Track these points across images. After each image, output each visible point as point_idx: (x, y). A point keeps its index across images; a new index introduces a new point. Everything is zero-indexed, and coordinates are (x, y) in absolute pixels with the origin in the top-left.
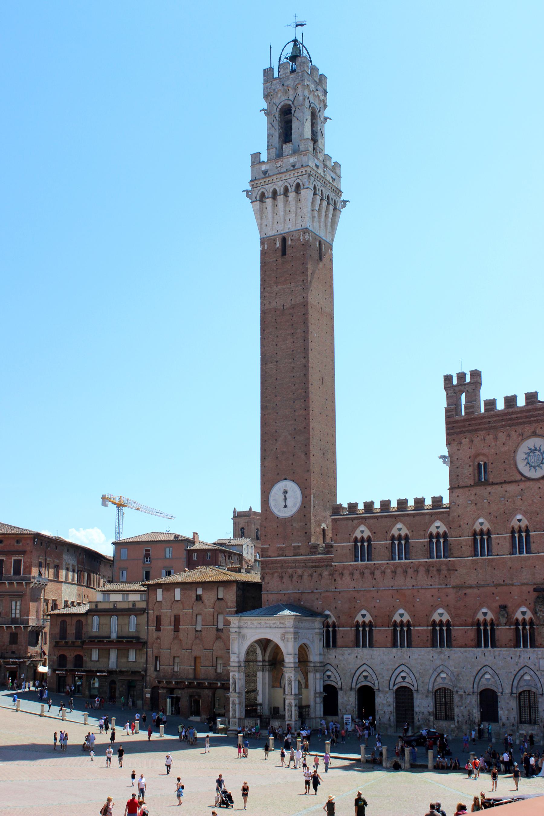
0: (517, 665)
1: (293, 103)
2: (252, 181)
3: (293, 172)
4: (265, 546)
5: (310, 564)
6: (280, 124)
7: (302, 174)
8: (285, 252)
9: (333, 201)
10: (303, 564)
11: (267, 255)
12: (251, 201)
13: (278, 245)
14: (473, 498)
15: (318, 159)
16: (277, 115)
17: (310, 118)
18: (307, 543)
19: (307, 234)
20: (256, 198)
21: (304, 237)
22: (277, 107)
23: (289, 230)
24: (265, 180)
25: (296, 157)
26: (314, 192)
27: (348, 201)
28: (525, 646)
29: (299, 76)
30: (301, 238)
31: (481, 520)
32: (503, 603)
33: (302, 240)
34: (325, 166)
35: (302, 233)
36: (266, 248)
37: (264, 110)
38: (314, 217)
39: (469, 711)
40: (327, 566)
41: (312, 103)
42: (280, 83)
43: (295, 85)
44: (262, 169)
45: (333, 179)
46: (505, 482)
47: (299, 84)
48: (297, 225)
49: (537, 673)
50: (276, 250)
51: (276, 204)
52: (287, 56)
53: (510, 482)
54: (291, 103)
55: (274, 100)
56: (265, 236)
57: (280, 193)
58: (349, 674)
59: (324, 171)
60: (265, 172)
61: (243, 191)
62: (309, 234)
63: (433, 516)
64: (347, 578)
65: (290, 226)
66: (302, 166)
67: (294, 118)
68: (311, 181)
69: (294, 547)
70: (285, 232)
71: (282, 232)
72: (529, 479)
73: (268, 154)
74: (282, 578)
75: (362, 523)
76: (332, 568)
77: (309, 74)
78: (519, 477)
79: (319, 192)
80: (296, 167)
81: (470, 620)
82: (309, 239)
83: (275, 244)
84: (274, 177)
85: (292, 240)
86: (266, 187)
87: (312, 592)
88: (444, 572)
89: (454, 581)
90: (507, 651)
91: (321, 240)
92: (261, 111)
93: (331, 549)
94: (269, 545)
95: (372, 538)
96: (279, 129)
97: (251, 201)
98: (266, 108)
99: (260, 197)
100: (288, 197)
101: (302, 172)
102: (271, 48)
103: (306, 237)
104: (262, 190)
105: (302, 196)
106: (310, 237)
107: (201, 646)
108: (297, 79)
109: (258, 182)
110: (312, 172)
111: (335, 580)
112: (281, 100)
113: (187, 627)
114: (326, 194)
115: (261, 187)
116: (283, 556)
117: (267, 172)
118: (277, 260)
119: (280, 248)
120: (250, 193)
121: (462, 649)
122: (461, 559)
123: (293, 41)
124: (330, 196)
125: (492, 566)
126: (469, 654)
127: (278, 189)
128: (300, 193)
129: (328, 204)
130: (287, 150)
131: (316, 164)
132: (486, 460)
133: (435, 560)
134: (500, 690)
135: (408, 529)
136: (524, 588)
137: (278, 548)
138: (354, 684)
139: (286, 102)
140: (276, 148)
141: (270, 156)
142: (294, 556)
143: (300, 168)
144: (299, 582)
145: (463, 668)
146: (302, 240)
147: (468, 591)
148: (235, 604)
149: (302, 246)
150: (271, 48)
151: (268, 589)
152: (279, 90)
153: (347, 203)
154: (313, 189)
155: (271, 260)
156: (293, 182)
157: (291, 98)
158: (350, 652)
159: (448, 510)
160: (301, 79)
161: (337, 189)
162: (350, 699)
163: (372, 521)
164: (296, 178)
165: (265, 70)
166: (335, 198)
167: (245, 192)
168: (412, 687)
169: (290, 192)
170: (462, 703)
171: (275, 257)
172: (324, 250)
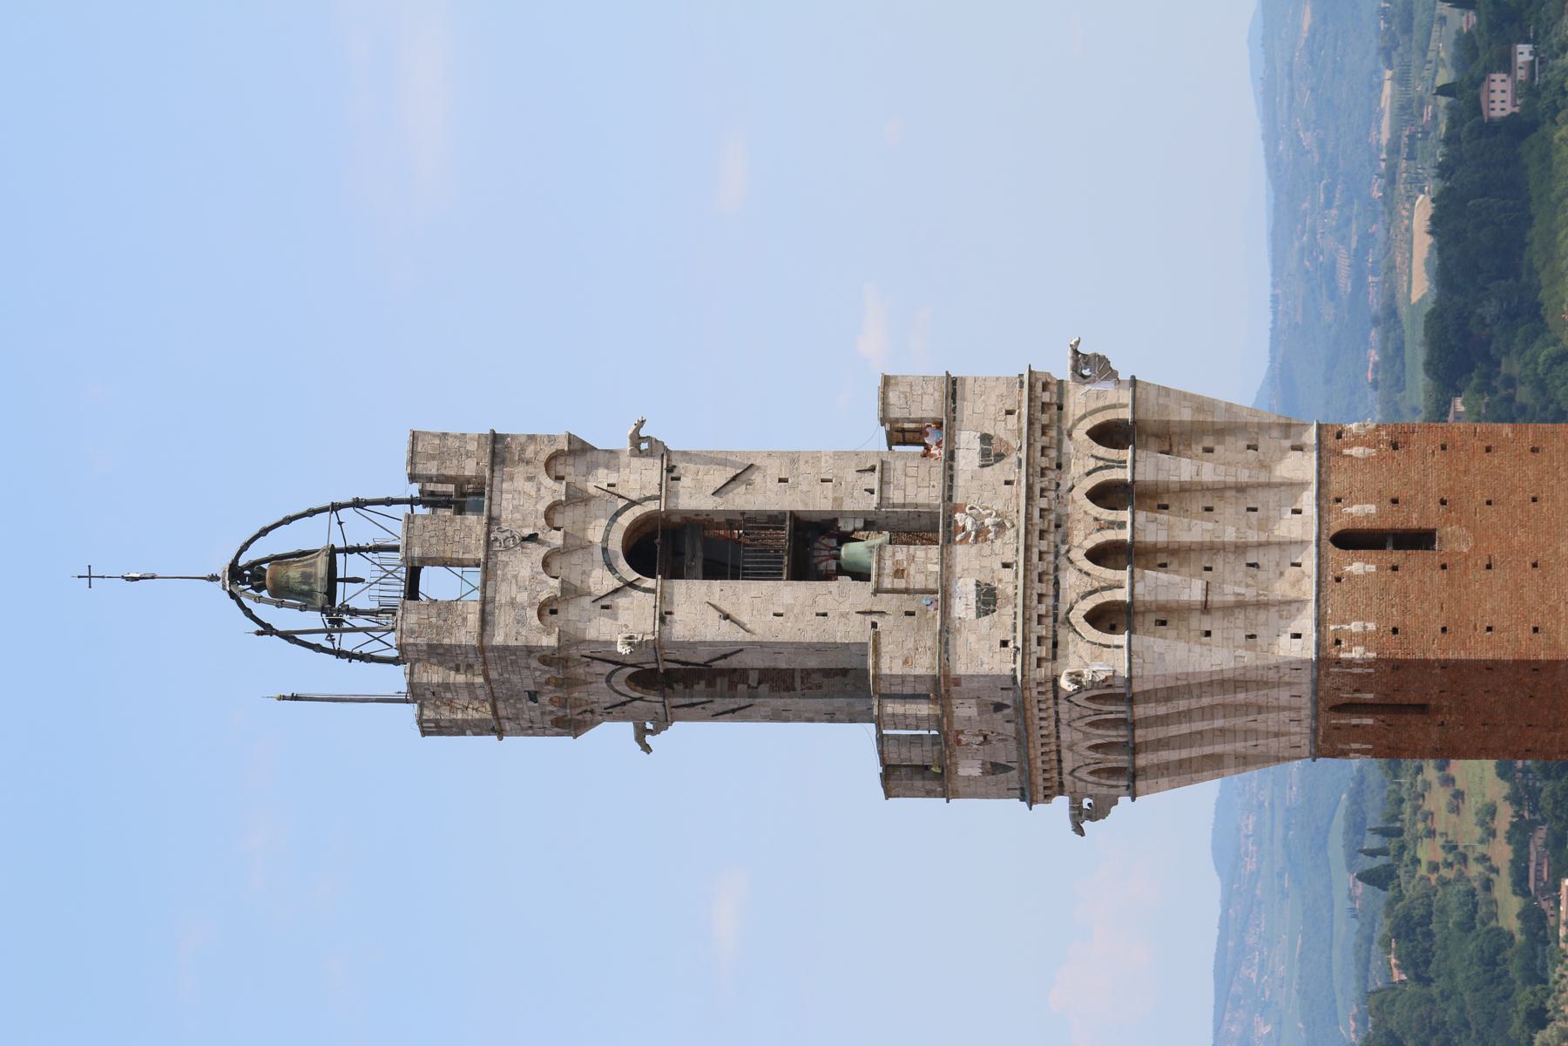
2: (1028, 795)
12: (1124, 801)
13: (1369, 721)
27: (1076, 352)
38: (1241, 605)
61: (1079, 830)
79: (1118, 584)
82: (1363, 638)
92: (647, 748)
97: (1124, 801)
98: (627, 728)
102: (295, 698)
120: (1086, 802)
150: (295, 698)
154: (1121, 639)
167: (1086, 825)
172: (1371, 508)
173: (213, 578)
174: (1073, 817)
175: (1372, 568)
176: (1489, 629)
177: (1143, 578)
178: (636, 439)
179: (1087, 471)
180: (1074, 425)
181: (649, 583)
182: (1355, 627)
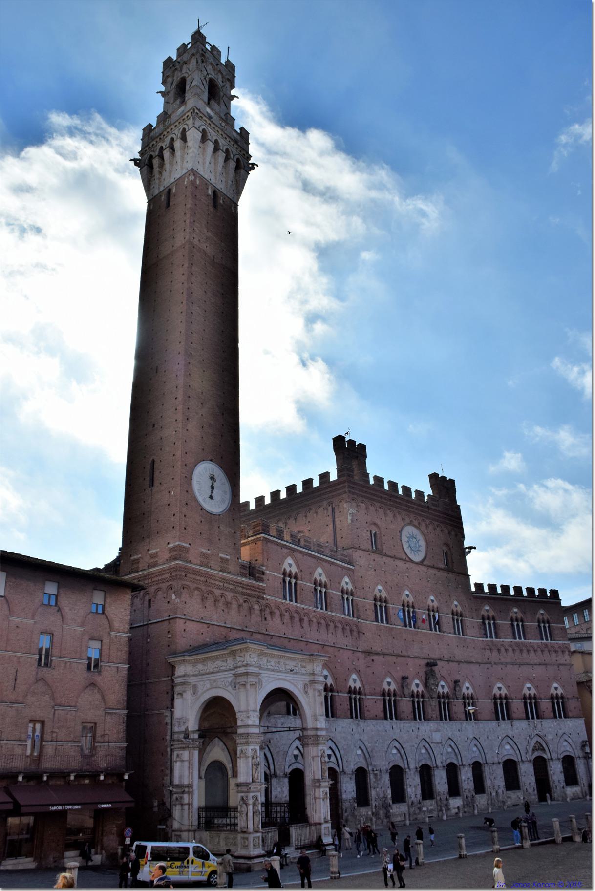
0: (417, 738)
4: (184, 545)
5: (240, 589)
10: (232, 587)
14: (372, 563)
16: (208, 80)
18: (237, 560)
22: (208, 74)
28: (420, 719)
30: (233, 208)
31: (380, 587)
32: (406, 675)
39: (384, 792)
40: (259, 597)
46: (394, 557)
49: (432, 745)
53: (400, 559)
58: (282, 753)
60: (210, 118)
63: (344, 571)
64: (277, 620)
69: (221, 558)
72: (411, 561)
74: (203, 599)
75: (290, 555)
76: (264, 602)
78: (404, 557)
81: (378, 690)
83: (207, 189)
87: (243, 630)
88: (355, 633)
89: (363, 646)
90: (410, 723)
93: (262, 576)
94: (190, 544)
95: (299, 577)
107: (47, 698)
111: (265, 619)
113: (19, 654)
116: (207, 566)
121: (374, 722)
122: (368, 622)
125: (392, 635)
126: (380, 726)
127: (221, 144)
132: (377, 530)
133: (351, 618)
134: (406, 766)
135: (327, 578)
136: (416, 660)
137: (202, 553)
138: (287, 767)
142: (221, 571)
144: (226, 610)
145: (376, 743)
147: (375, 657)
148: (128, 627)
151: (185, 613)
158: (283, 721)
159: (353, 568)
162: (284, 789)
163: (299, 556)
168: (337, 769)
170: (378, 784)
171: (206, 201)
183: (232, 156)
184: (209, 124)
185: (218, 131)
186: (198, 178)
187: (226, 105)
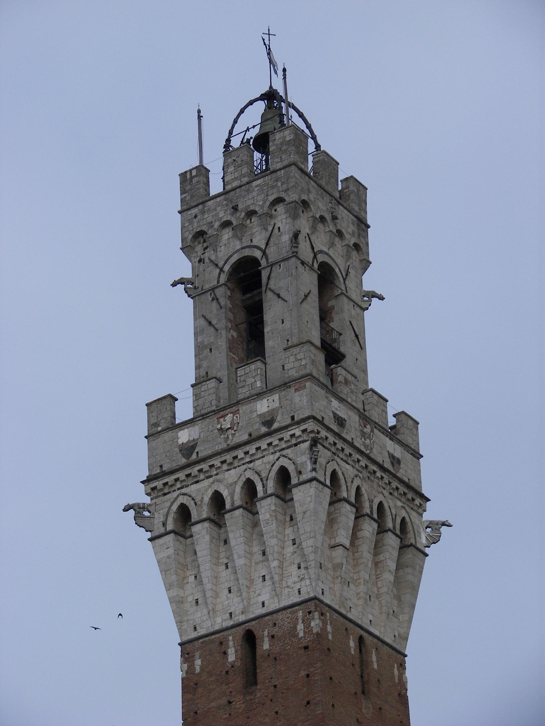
1: (264, 252)
3: (269, 440)
6: (231, 315)
7: (294, 441)
8: (255, 674)
9: (398, 521)
11: (200, 690)
12: (149, 535)
13: (232, 657)
15: (341, 400)
17: (315, 291)
19: (316, 615)
20: (164, 524)
21: (307, 626)
22: (221, 270)
23: (264, 611)
24: (187, 471)
25: (276, 397)
26: (334, 494)
27: (444, 524)
29: (277, 180)
30: (300, 627)
33: (301, 634)
34: (365, 418)
35: (300, 614)
36: (198, 670)
37: (182, 281)
41: (321, 252)
42: (227, 205)
43: (268, 203)
44: (180, 442)
45: (396, 461)
47: (279, 200)
48: (287, 590)
50: (227, 672)
51: (223, 537)
52: (248, 136)
54: (258, 254)
55: (210, 254)
56: (194, 635)
57: (233, 504)
59: (363, 434)
61: (126, 509)
62: (322, 614)
65: (265, 597)
66: (293, 418)
67: (269, 294)
68: (322, 461)
70: (252, 616)
71: (242, 618)
73: (197, 396)
77: (304, 172)
80: (276, 426)
82: (324, 629)
83: (225, 653)
84: (216, 462)
85: (273, 637)
86: (193, 489)
91: (365, 635)
92: (174, 285)
96: (228, 330)
97: (149, 535)
98: (188, 275)
99: (175, 520)
100: (257, 513)
101: (293, 436)
102: (200, 117)
103: (313, 624)
104: (183, 500)
105: (297, 505)
106: (324, 623)
108: (273, 187)
109: (170, 479)
110: (324, 433)
112: (231, 251)
114: (371, 501)
115: (178, 492)
117: (193, 447)
118: (230, 702)
119: (238, 664)
123: (262, 98)
124: (386, 505)
127: (225, 493)
128: (292, 499)
129: (382, 530)
130: (250, 380)
131: (335, 414)
139: (247, 252)
140: (220, 381)
141: (201, 402)
143: (285, 428)
146: (301, 634)
149: (302, 651)
150: (200, 117)
152: (226, 224)
153: (444, 529)
154: (328, 483)
155: (213, 704)
156: (268, 467)
157: (259, 240)
160: (285, 187)
161: (409, 486)
164: (278, 454)
165: (183, 176)
166: (404, 514)
167: (132, 512)
169: (263, 498)
172: (375, 667)
173: (271, 87)
174: (138, 504)
175: (353, 652)
176: (333, 705)
177: (352, 512)
178: (373, 295)
179: (391, 507)
180: (407, 512)
181: (316, 266)
182: (329, 629)
183: (259, 488)
184: (188, 476)
185: (212, 466)
186: (197, 654)
187: (279, 296)
